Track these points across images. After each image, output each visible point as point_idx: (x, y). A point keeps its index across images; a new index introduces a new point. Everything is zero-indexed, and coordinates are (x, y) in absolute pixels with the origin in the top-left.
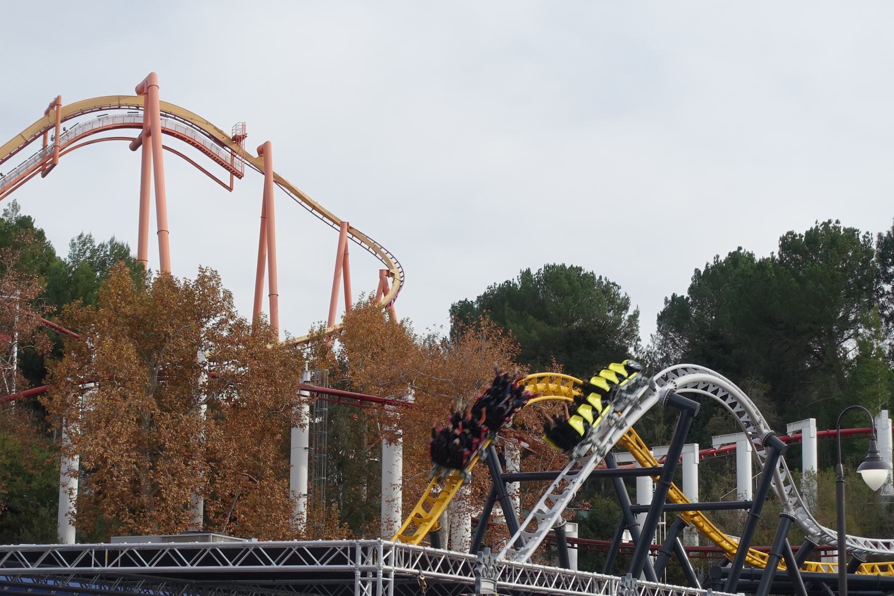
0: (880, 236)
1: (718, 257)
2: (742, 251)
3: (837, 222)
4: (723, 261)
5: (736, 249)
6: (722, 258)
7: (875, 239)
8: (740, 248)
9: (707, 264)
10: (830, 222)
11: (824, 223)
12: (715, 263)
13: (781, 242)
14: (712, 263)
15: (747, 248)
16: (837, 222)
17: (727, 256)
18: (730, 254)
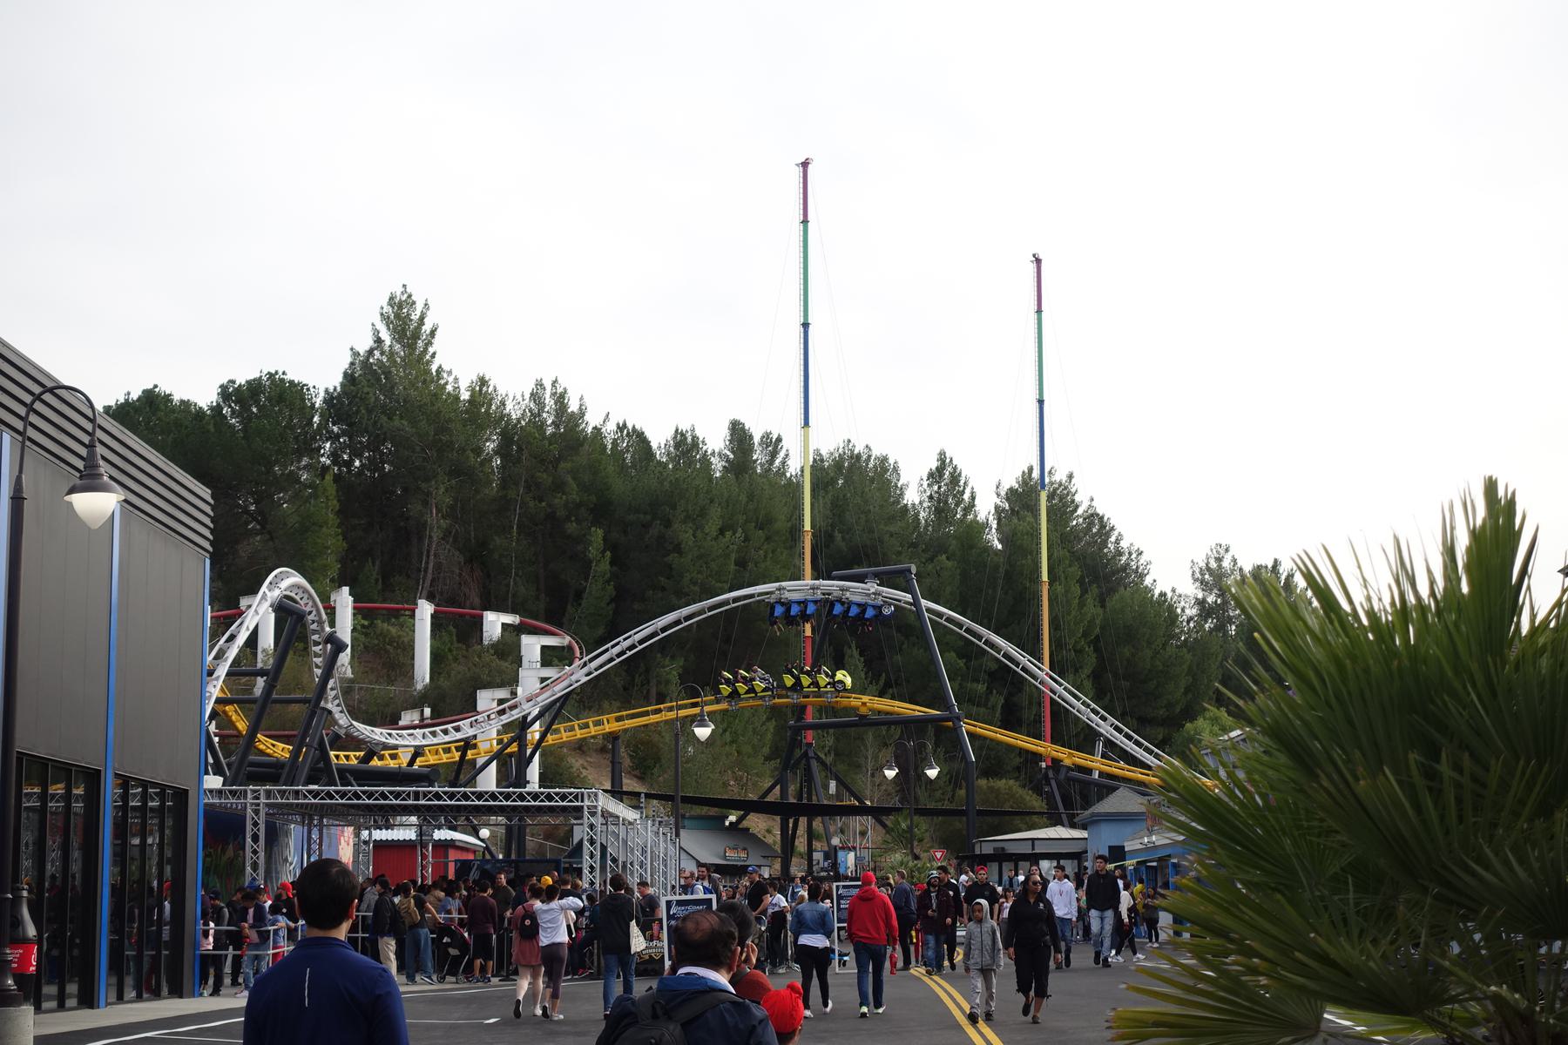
0: (327, 391)
1: (129, 394)
2: (157, 390)
3: (284, 373)
4: (135, 399)
5: (151, 387)
6: (135, 396)
7: (322, 394)
8: (156, 386)
9: (117, 401)
10: (277, 373)
11: (269, 373)
12: (125, 400)
13: (220, 390)
14: (122, 400)
15: (165, 387)
16: (284, 373)
17: (140, 393)
18: (144, 391)
